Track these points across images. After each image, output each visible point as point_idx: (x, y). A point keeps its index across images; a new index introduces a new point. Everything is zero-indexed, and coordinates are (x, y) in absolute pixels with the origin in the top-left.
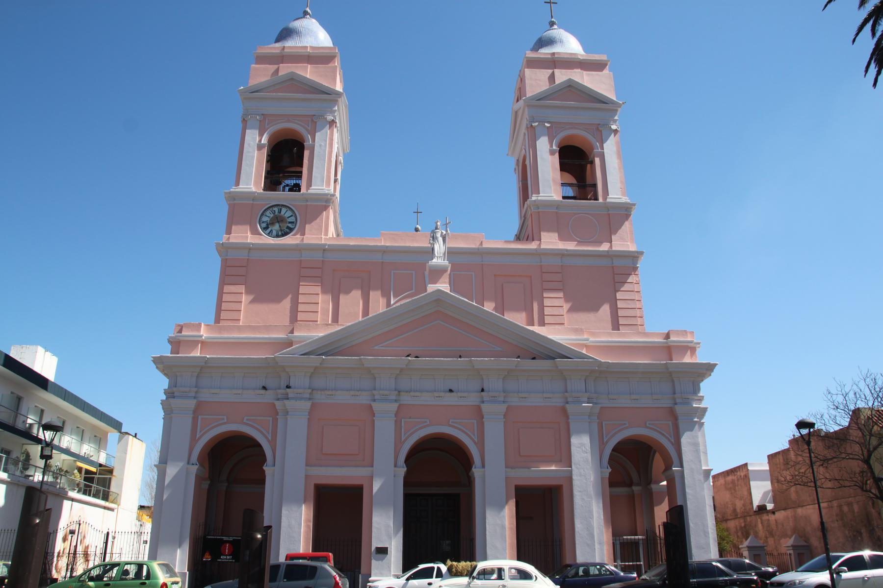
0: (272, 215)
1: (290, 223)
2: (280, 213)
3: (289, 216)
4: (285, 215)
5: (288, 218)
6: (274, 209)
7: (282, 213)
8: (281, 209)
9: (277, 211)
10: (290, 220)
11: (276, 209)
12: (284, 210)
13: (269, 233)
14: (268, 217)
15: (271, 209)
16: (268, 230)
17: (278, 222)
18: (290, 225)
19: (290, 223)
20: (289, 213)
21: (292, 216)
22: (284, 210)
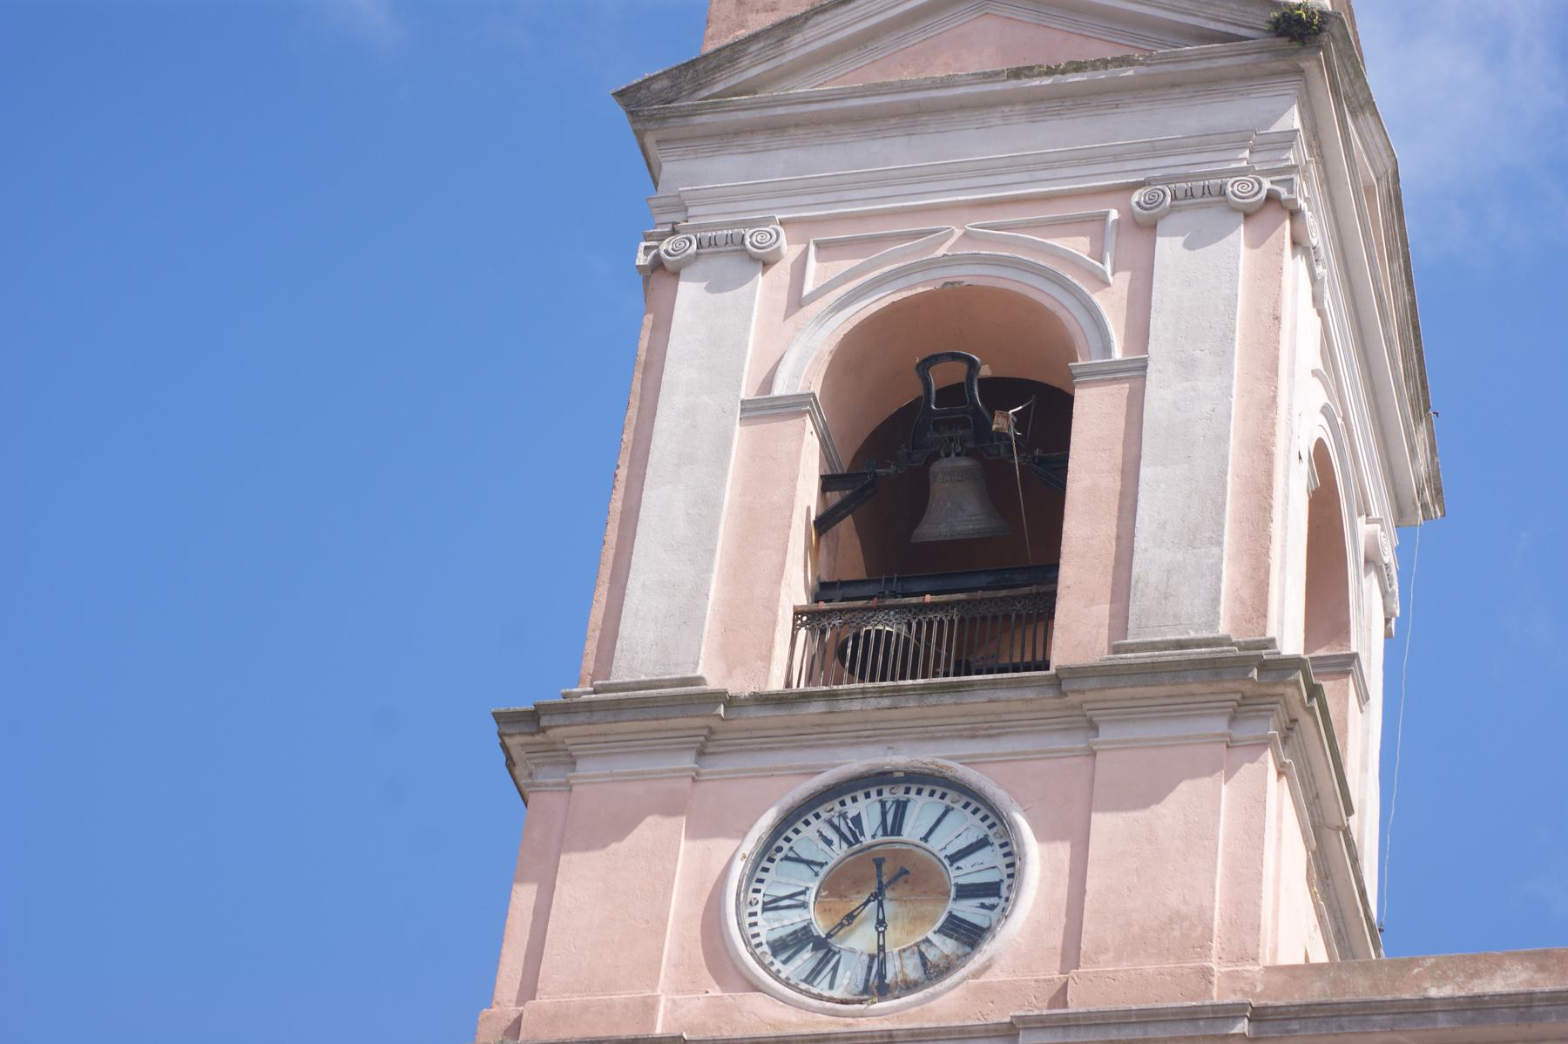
0: (839, 851)
1: (965, 892)
2: (897, 828)
3: (962, 843)
4: (935, 844)
5: (955, 858)
6: (852, 810)
7: (913, 829)
8: (901, 807)
9: (871, 823)
10: (971, 871)
11: (867, 810)
12: (921, 811)
14: (809, 863)
15: (826, 811)
18: (968, 910)
19: (965, 892)
20: (961, 828)
22: (921, 811)
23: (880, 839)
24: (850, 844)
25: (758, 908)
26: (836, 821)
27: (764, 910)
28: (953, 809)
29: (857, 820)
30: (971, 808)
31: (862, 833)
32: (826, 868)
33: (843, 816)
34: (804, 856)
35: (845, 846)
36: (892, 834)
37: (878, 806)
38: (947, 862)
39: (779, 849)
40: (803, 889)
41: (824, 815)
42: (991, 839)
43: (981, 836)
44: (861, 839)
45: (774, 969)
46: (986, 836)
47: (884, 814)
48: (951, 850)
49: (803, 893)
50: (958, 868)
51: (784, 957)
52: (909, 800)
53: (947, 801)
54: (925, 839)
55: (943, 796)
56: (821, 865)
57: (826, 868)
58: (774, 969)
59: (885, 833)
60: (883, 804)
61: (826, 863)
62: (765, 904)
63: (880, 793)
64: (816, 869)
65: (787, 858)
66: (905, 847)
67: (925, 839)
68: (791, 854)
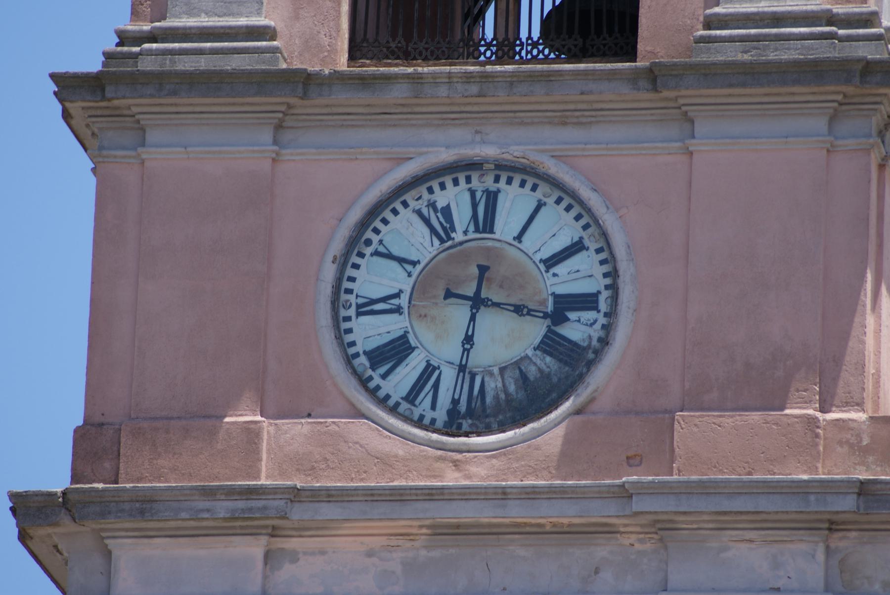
6: (442, 199)
8: (492, 198)
13: (412, 396)
15: (417, 199)
16: (401, 371)
17: (477, 302)
21: (576, 248)
23: (471, 235)
24: (442, 241)
25: (352, 312)
26: (425, 211)
27: (359, 314)
28: (545, 204)
29: (447, 212)
30: (564, 204)
31: (453, 229)
32: (419, 268)
33: (432, 205)
34: (396, 252)
35: (436, 242)
36: (484, 231)
37: (467, 196)
38: (542, 267)
39: (368, 242)
40: (397, 291)
41: (413, 204)
42: (587, 242)
43: (576, 239)
44: (453, 235)
45: (372, 385)
46: (581, 238)
47: (475, 206)
48: (546, 253)
49: (397, 295)
50: (555, 275)
51: (383, 370)
52: (499, 191)
53: (539, 194)
54: (519, 238)
55: (534, 188)
56: (414, 263)
57: (419, 268)
58: (372, 385)
59: (477, 230)
60: (473, 193)
61: (419, 262)
62: (359, 306)
63: (468, 180)
64: (409, 268)
65: (376, 253)
66: (497, 244)
67: (519, 238)
68: (381, 249)
